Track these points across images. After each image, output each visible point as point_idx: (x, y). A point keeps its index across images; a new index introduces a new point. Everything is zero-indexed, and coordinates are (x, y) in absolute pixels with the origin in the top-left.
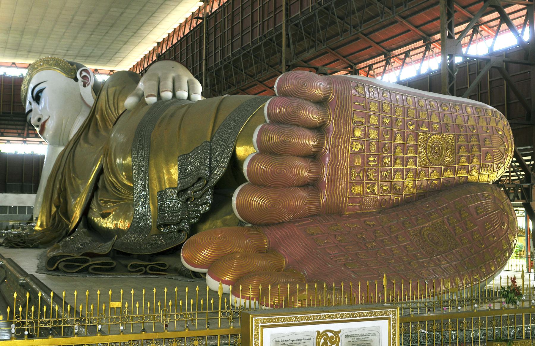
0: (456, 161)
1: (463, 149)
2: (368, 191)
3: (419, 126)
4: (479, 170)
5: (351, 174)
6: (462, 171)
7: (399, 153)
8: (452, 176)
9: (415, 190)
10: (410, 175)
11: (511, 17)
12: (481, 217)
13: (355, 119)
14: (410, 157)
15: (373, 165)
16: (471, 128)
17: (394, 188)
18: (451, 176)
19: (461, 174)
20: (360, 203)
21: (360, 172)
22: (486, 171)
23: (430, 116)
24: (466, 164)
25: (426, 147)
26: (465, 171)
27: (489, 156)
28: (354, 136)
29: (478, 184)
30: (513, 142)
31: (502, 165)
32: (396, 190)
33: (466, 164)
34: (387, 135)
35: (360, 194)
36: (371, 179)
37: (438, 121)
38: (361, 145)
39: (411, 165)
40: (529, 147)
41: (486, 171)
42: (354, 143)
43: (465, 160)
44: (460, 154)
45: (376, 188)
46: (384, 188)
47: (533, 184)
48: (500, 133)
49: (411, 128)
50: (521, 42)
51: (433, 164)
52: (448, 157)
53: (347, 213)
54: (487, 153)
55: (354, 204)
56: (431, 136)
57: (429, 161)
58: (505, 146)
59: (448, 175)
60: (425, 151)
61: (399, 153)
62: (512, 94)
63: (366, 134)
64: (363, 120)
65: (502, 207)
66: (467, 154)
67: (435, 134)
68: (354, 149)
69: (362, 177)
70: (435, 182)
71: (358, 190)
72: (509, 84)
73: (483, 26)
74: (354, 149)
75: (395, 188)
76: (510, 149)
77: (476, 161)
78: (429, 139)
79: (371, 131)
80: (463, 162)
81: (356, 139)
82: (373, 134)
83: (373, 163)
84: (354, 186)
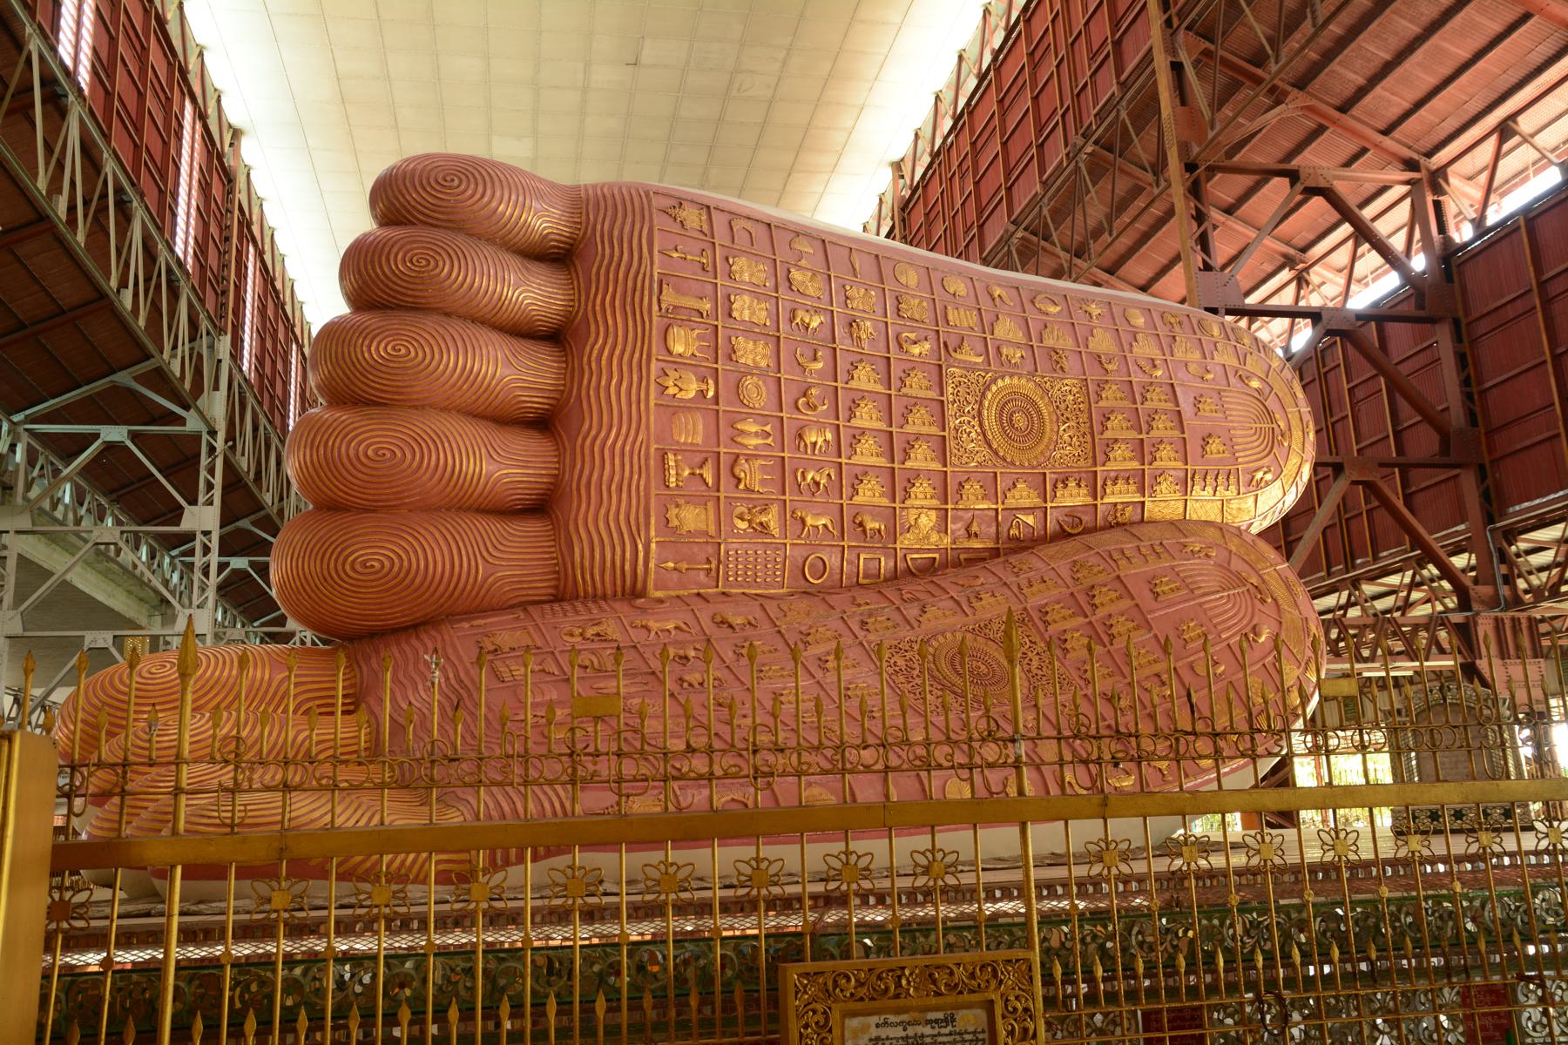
0: (1094, 457)
1: (1116, 422)
2: (743, 525)
3: (945, 348)
4: (1185, 484)
5: (664, 468)
6: (1121, 485)
7: (867, 417)
8: (1089, 500)
9: (947, 541)
10: (922, 489)
11: (1368, 213)
12: (1169, 607)
13: (669, 297)
14: (918, 437)
15: (756, 447)
16: (1142, 363)
17: (850, 524)
18: (1079, 501)
19: (1120, 495)
20: (709, 562)
21: (701, 467)
22: (1209, 489)
23: (987, 327)
24: (1135, 465)
25: (980, 413)
26: (1133, 488)
27: (1215, 446)
28: (670, 353)
29: (1180, 526)
30: (1308, 418)
31: (1269, 477)
32: (864, 531)
33: (1135, 465)
34: (815, 359)
35: (706, 533)
36: (748, 490)
37: (1020, 337)
38: (703, 380)
39: (923, 458)
40: (1462, 527)
41: (1209, 489)
42: (671, 373)
43: (1128, 454)
44: (1108, 434)
45: (771, 518)
46: (809, 521)
47: (1478, 614)
48: (1255, 384)
49: (916, 350)
50: (1408, 277)
51: (1013, 463)
52: (1066, 447)
53: (659, 594)
54: (1210, 435)
55: (684, 566)
56: (994, 381)
57: (996, 453)
58: (1272, 420)
59: (1073, 497)
60: (975, 422)
61: (867, 417)
62: (1403, 405)
63: (718, 349)
64: (707, 306)
65: (1254, 580)
66: (1133, 434)
67: (1011, 376)
68: (672, 391)
69: (710, 481)
70: (1030, 520)
71: (691, 518)
72: (1395, 387)
73: (1316, 268)
74: (672, 391)
75: (861, 524)
76: (1297, 434)
77: (1167, 458)
78: (988, 388)
79: (741, 342)
80: (1122, 459)
81: (679, 363)
82: (753, 353)
83: (754, 442)
84: (678, 506)
